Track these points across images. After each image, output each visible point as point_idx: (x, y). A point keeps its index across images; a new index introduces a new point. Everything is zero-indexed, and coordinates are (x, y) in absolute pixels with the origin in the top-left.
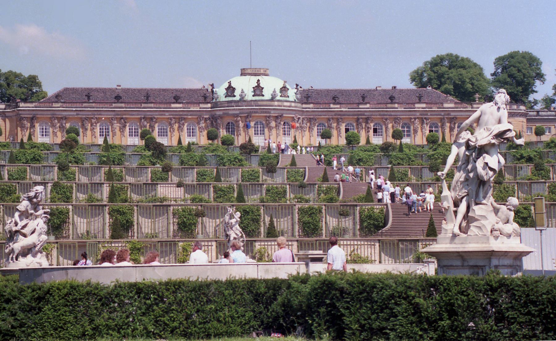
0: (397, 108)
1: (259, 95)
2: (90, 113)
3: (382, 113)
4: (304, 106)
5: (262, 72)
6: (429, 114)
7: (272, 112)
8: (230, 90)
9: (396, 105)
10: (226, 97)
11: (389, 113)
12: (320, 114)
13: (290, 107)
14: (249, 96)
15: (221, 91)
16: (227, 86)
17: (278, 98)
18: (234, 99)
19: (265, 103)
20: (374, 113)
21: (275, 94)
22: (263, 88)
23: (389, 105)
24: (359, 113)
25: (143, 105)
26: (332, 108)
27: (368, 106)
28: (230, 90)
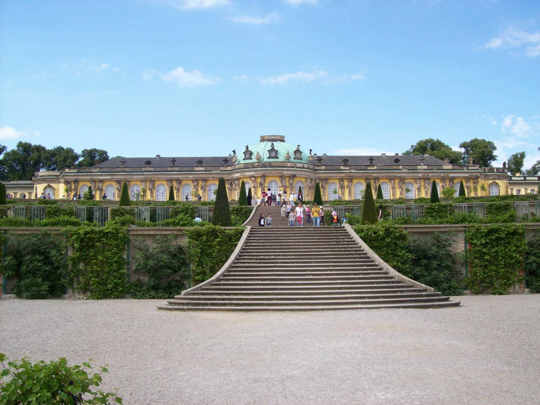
0: (401, 170)
1: (273, 158)
2: (123, 177)
3: (388, 175)
5: (279, 138)
6: (430, 175)
7: (285, 173)
8: (248, 154)
9: (401, 167)
10: (244, 159)
11: (394, 175)
12: (331, 175)
15: (240, 156)
16: (244, 150)
17: (292, 160)
18: (251, 161)
20: (381, 175)
23: (395, 167)
24: (368, 174)
25: (169, 169)
27: (375, 167)
28: (248, 154)
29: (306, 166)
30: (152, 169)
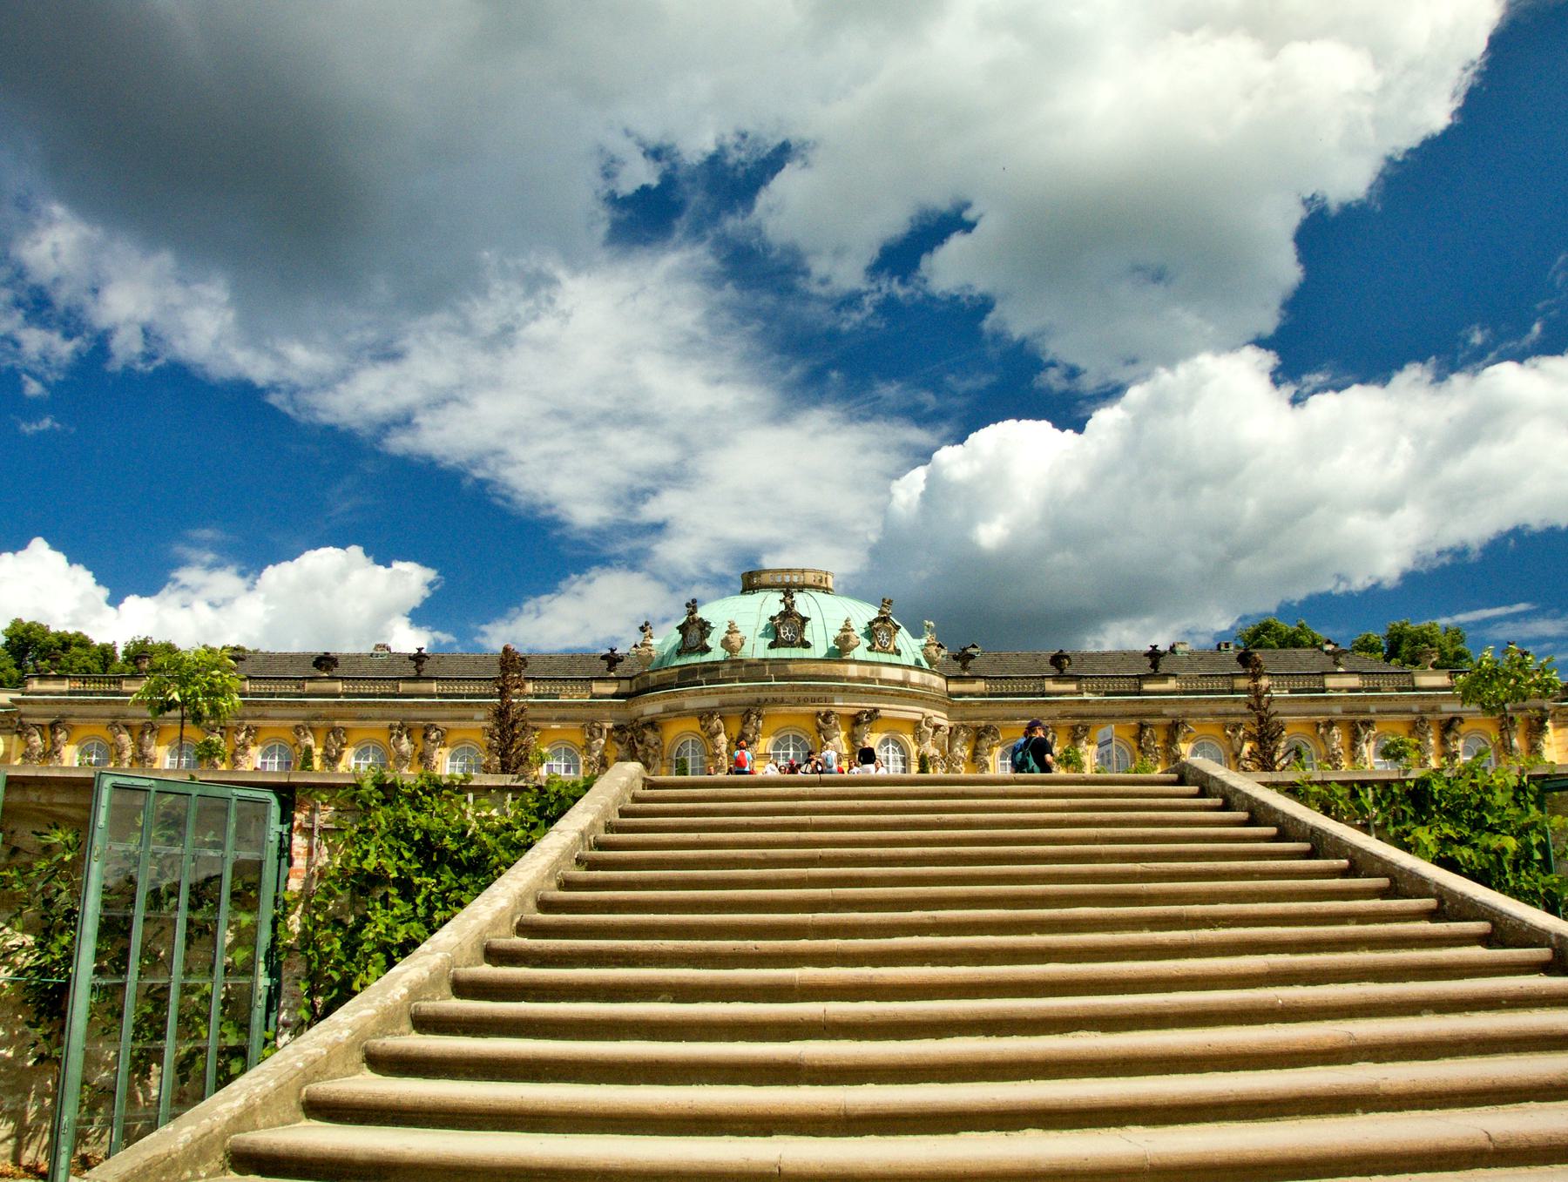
1: (789, 644)
3: (1220, 708)
4: (953, 687)
5: (810, 579)
13: (903, 683)
14: (756, 648)
15: (665, 639)
17: (860, 653)
18: (707, 658)
19: (812, 669)
21: (847, 638)
22: (805, 620)
24: (1146, 708)
25: (402, 687)
26: (1050, 694)
27: (1171, 684)
28: (694, 631)
29: (915, 677)
30: (339, 686)
